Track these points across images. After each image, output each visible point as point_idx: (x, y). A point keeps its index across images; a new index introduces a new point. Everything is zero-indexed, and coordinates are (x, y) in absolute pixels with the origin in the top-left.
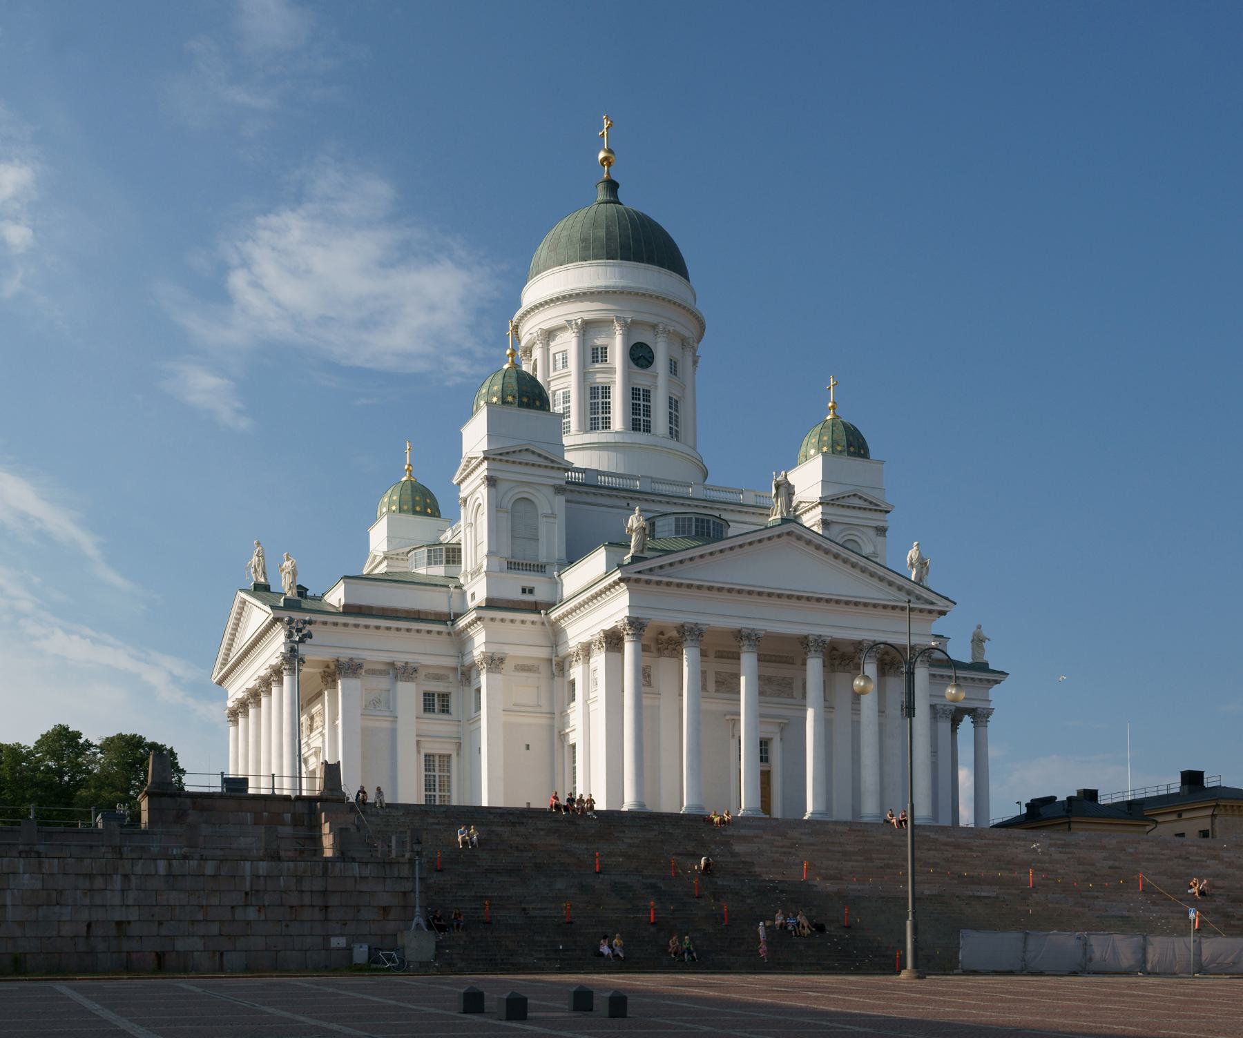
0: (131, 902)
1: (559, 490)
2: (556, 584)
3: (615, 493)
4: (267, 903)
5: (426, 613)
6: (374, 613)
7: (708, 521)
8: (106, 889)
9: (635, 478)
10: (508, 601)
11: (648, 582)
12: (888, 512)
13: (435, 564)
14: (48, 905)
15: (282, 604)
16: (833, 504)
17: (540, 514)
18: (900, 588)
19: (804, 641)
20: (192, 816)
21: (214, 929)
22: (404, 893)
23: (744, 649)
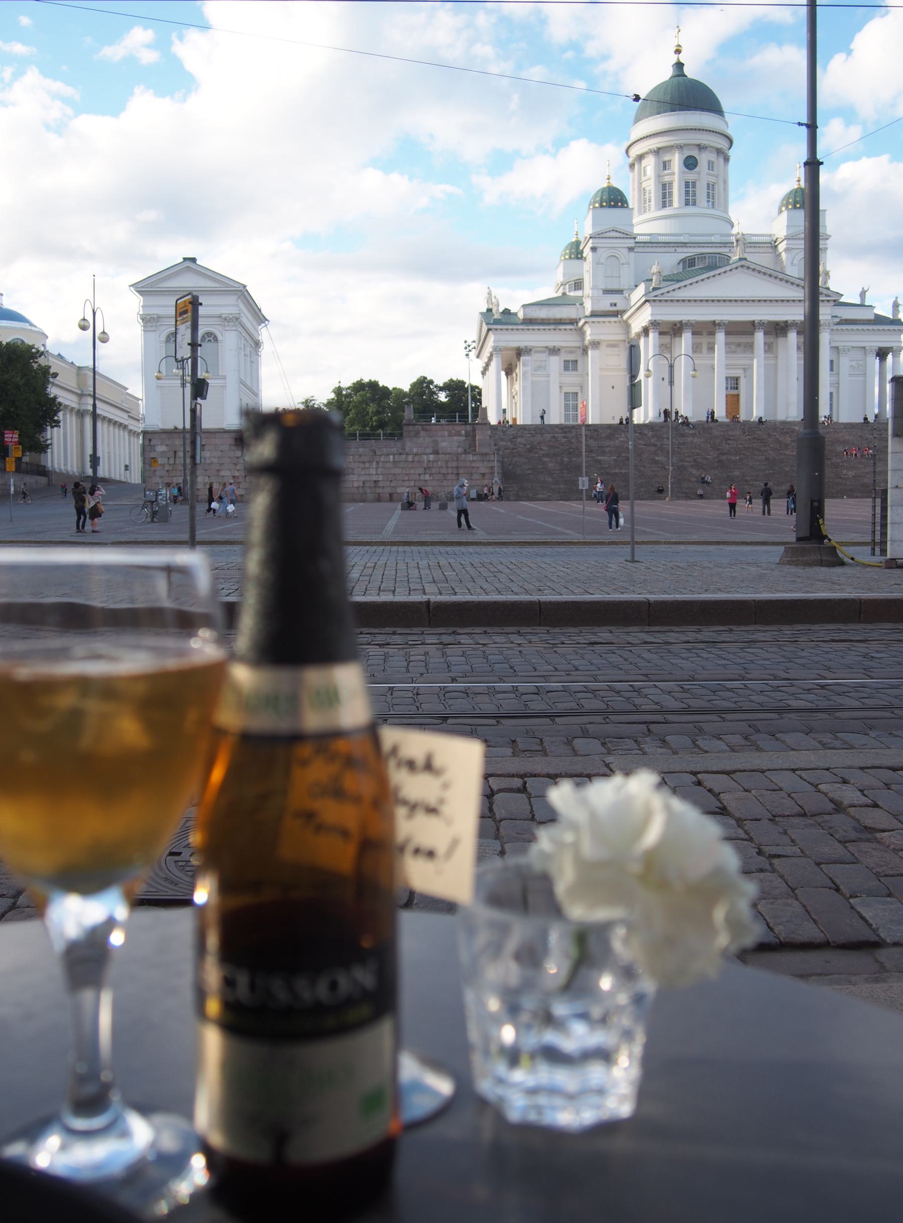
0: (379, 473)
1: (631, 249)
2: (628, 300)
3: (667, 245)
4: (433, 472)
5: (565, 319)
6: (538, 322)
7: (716, 257)
9: (681, 235)
10: (603, 311)
11: (660, 301)
12: (827, 239)
13: (578, 289)
15: (492, 322)
16: (793, 239)
17: (621, 262)
20: (422, 433)
21: (412, 484)
22: (492, 467)
23: (717, 331)
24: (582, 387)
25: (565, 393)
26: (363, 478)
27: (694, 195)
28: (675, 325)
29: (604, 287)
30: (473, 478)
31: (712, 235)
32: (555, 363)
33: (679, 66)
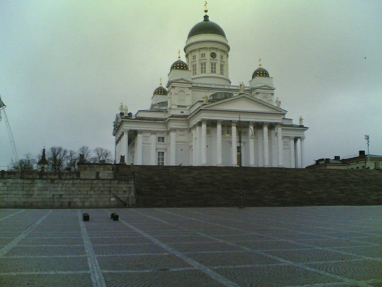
0: (63, 190)
1: (190, 88)
5: (159, 118)
8: (58, 187)
10: (177, 115)
11: (207, 110)
12: (274, 90)
14: (45, 190)
18: (273, 109)
19: (248, 123)
20: (88, 168)
21: (83, 196)
24: (166, 149)
25: (158, 152)
26: (53, 193)
27: (215, 68)
28: (213, 122)
29: (178, 104)
30: (118, 193)
31: (224, 86)
32: (153, 138)
33: (206, 17)
